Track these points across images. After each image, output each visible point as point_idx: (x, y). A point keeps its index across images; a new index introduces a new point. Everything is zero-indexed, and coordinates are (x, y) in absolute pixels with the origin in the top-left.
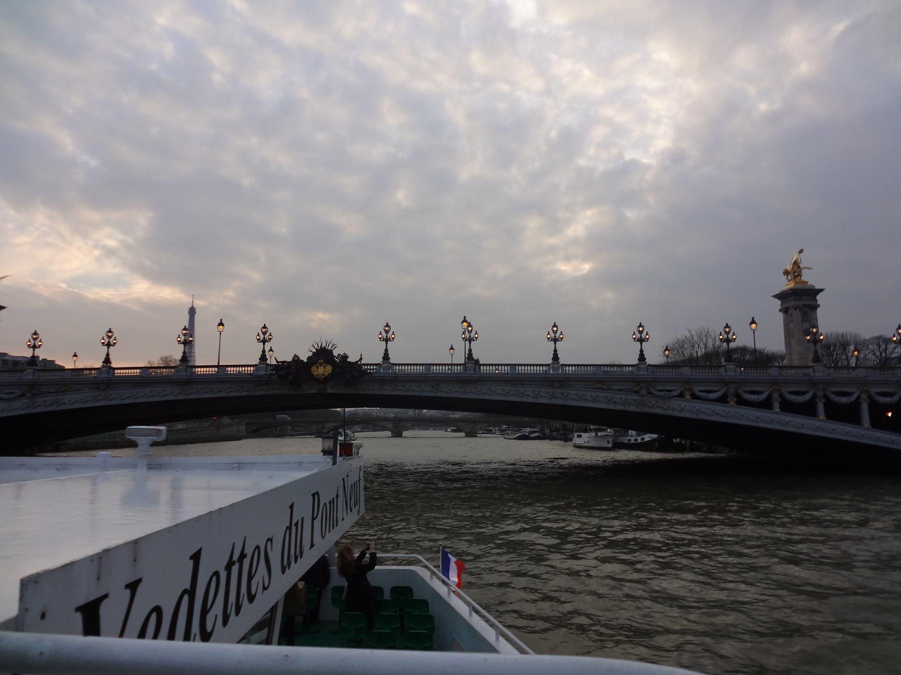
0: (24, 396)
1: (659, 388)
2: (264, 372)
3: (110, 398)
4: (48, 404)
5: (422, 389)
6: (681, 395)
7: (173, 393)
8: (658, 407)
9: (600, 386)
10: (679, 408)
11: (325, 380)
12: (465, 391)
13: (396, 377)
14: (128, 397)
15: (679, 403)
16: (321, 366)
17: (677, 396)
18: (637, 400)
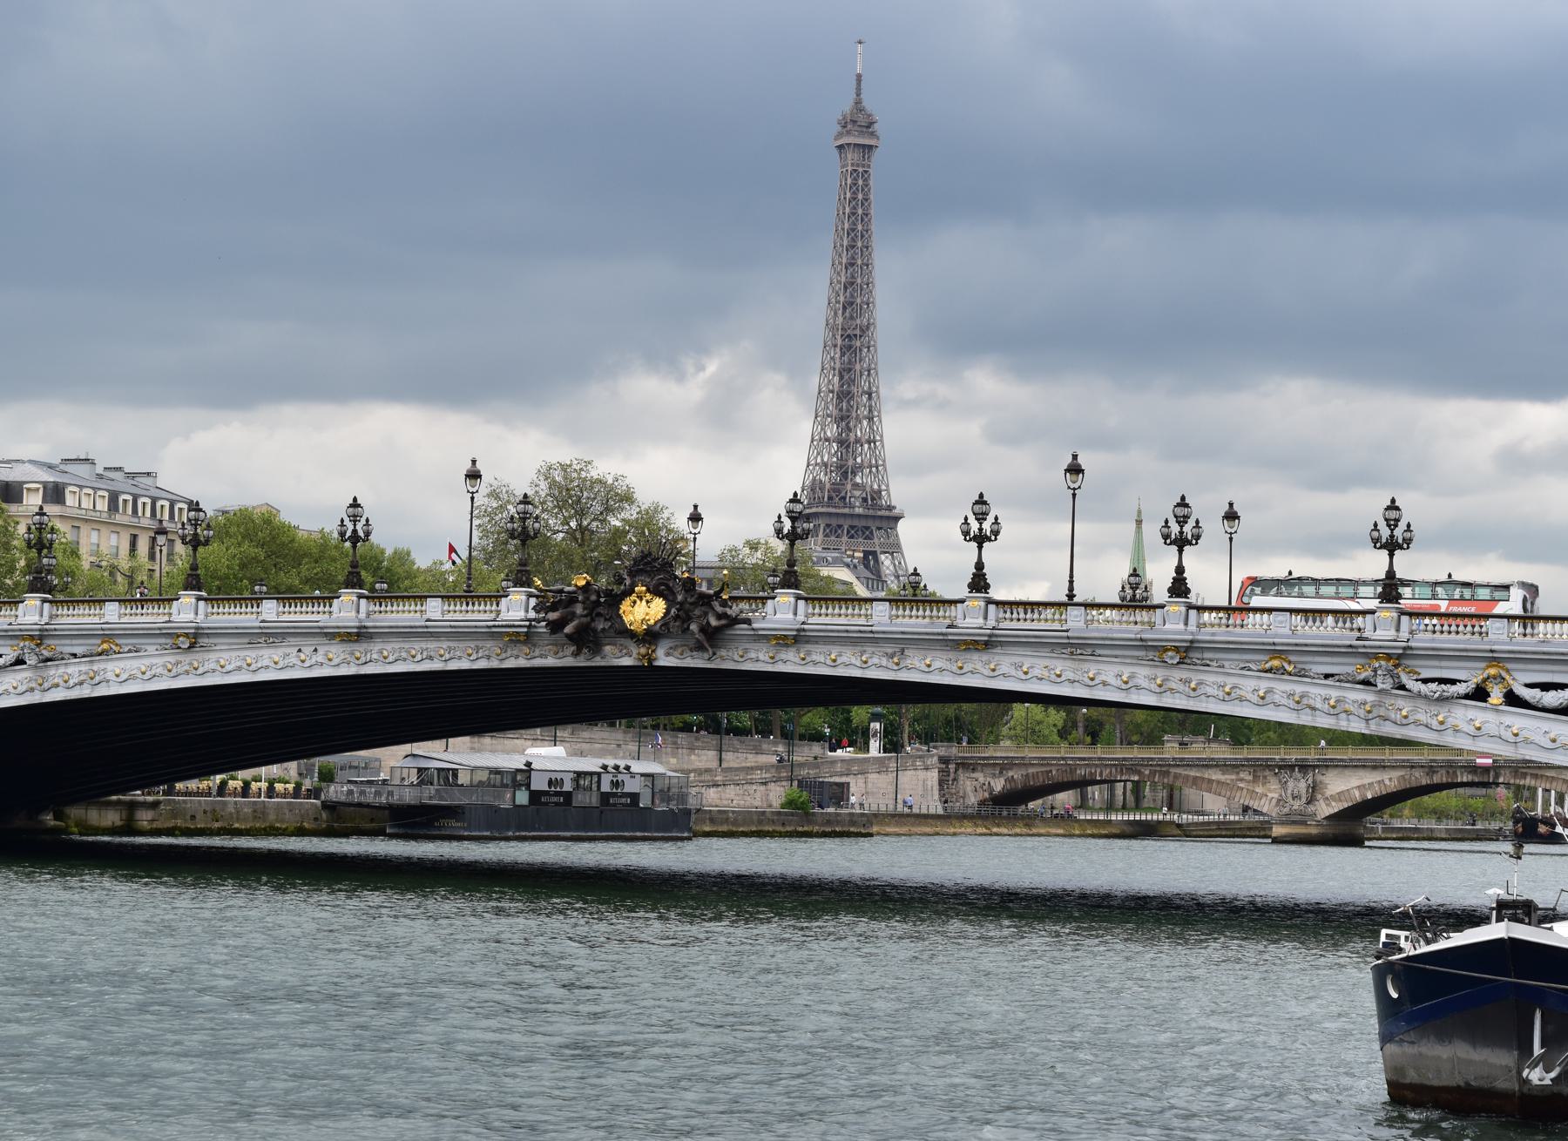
0: (25, 663)
1: (1426, 674)
2: (521, 614)
3: (201, 670)
4: (71, 683)
5: (866, 662)
6: (1480, 694)
7: (330, 660)
8: (1417, 723)
9: (1276, 663)
10: (1471, 730)
11: (651, 636)
12: (961, 668)
13: (804, 630)
14: (239, 669)
15: (1471, 714)
16: (641, 600)
17: (1467, 697)
18: (1365, 703)
